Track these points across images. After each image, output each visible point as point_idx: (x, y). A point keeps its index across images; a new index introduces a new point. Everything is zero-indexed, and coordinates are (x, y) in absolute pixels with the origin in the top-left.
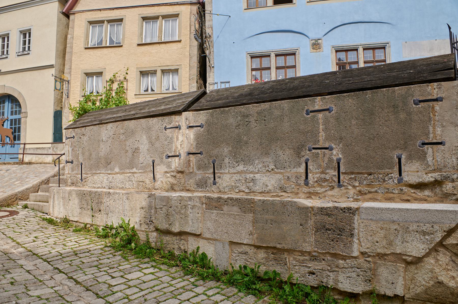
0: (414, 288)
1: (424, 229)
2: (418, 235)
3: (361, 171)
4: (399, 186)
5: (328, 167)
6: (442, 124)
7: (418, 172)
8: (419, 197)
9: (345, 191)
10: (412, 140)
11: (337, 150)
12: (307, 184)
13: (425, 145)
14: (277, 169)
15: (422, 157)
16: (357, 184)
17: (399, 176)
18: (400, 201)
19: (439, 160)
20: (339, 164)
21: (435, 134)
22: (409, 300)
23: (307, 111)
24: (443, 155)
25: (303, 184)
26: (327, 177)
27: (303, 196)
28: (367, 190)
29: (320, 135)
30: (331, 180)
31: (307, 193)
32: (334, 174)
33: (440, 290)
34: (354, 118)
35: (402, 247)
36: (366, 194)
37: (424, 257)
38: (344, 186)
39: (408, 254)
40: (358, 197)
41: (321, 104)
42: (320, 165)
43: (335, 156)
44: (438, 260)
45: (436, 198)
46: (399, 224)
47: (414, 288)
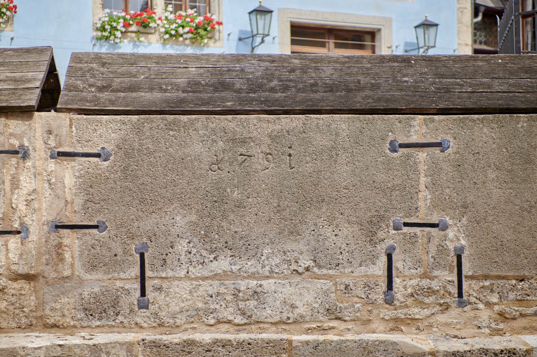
3: (503, 274)
5: (437, 265)
9: (472, 314)
11: (456, 229)
12: (389, 301)
14: (320, 267)
16: (494, 299)
20: (459, 257)
23: (392, 143)
25: (381, 302)
26: (435, 285)
27: (382, 328)
28: (517, 311)
29: (420, 196)
30: (442, 292)
31: (391, 319)
32: (450, 279)
34: (493, 166)
36: (514, 319)
38: (470, 303)
40: (498, 324)
41: (424, 131)
42: (419, 261)
43: (452, 241)
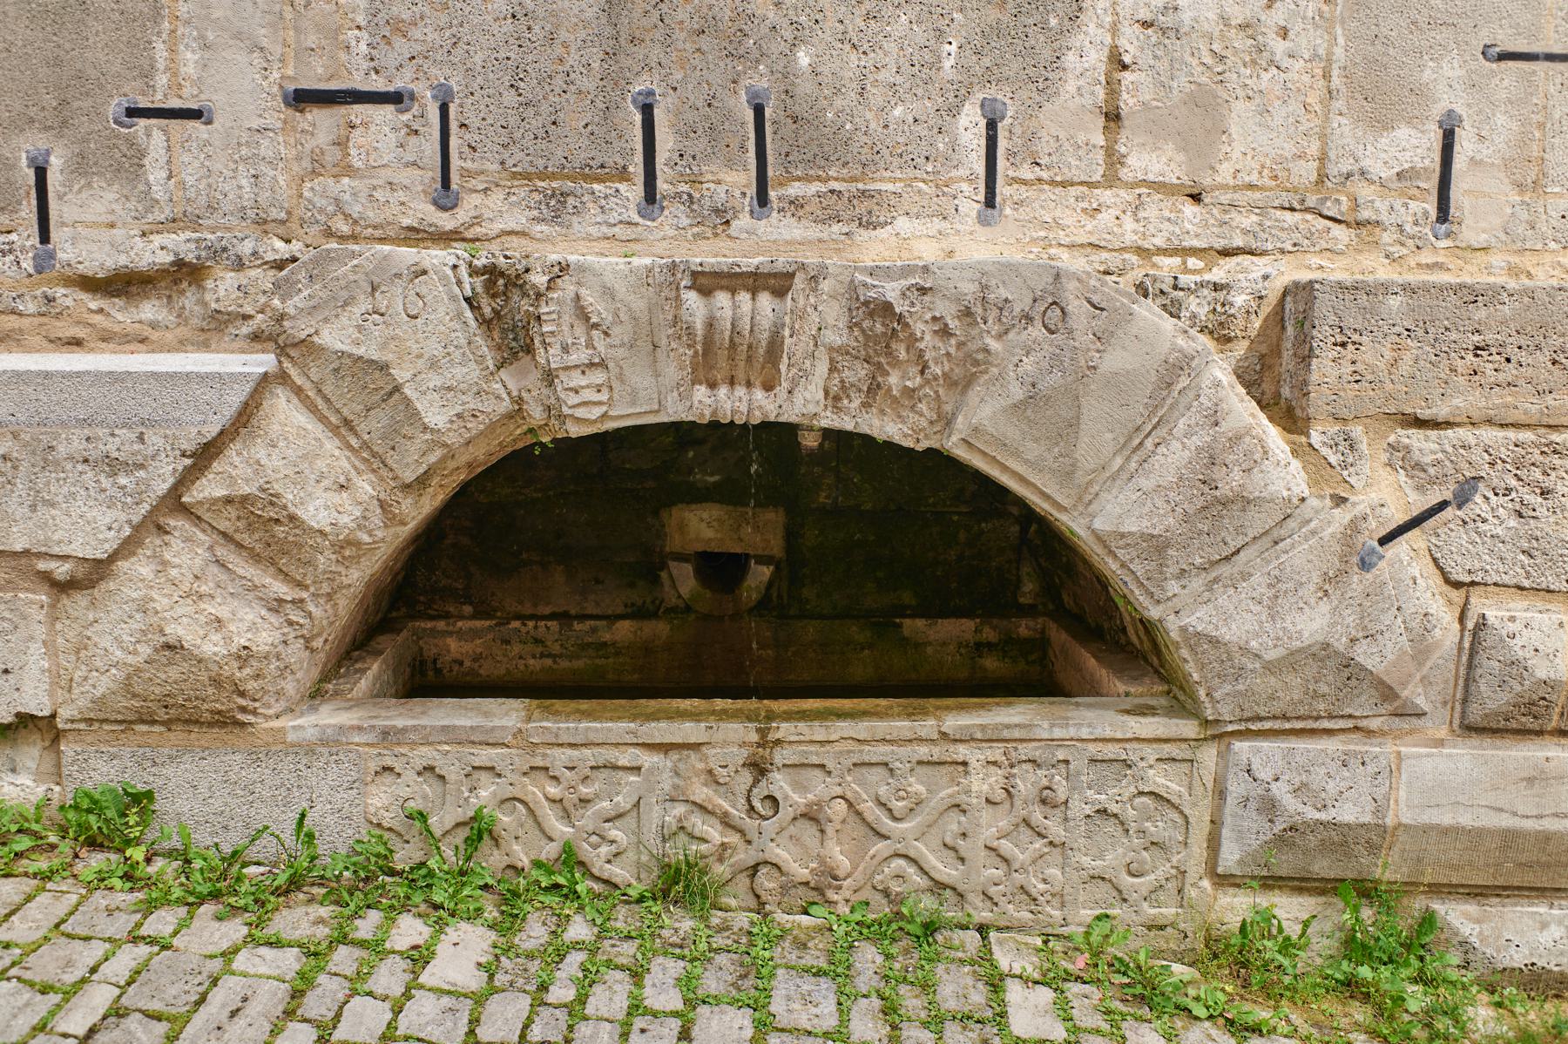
0: (86, 679)
1: (111, 447)
2: (90, 474)
4: (39, 284)
6: (202, 37)
7: (112, 226)
8: (117, 328)
10: (87, 94)
13: (140, 117)
15: (130, 165)
17: (41, 243)
18: (45, 344)
19: (190, 180)
21: (175, 75)
22: (75, 726)
24: (207, 163)
33: (174, 673)
35: (31, 523)
37: (113, 557)
39: (56, 550)
44: (165, 563)
45: (183, 332)
46: (15, 436)
47: (86, 679)
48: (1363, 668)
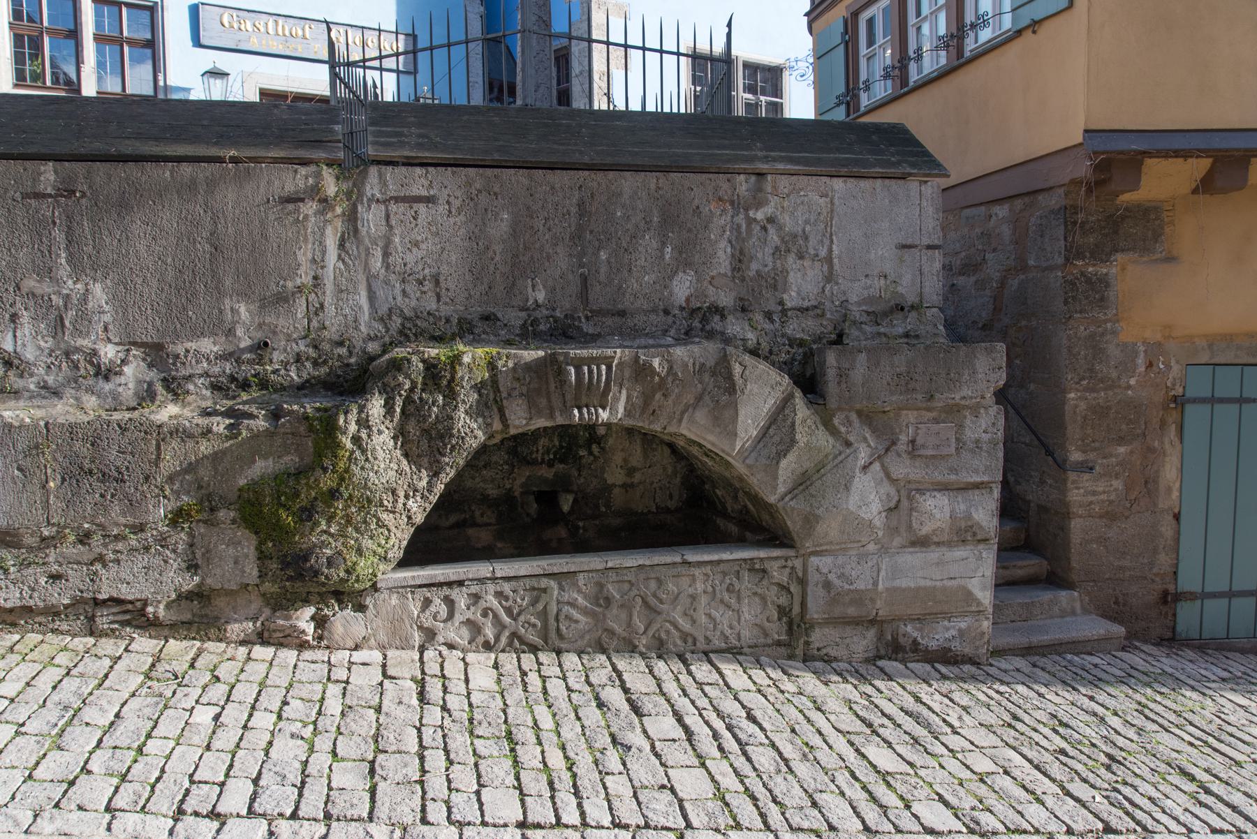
48: (864, 519)
